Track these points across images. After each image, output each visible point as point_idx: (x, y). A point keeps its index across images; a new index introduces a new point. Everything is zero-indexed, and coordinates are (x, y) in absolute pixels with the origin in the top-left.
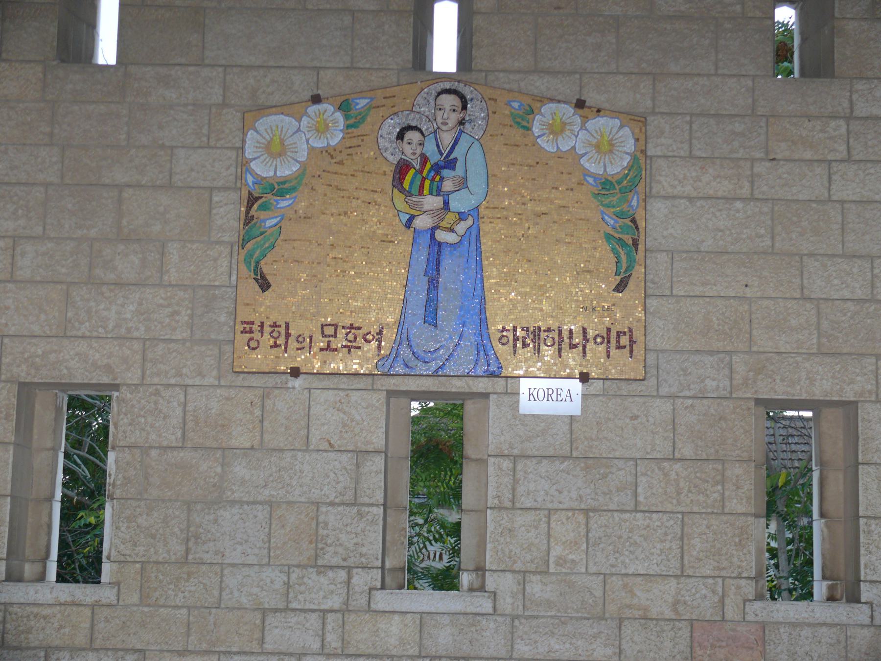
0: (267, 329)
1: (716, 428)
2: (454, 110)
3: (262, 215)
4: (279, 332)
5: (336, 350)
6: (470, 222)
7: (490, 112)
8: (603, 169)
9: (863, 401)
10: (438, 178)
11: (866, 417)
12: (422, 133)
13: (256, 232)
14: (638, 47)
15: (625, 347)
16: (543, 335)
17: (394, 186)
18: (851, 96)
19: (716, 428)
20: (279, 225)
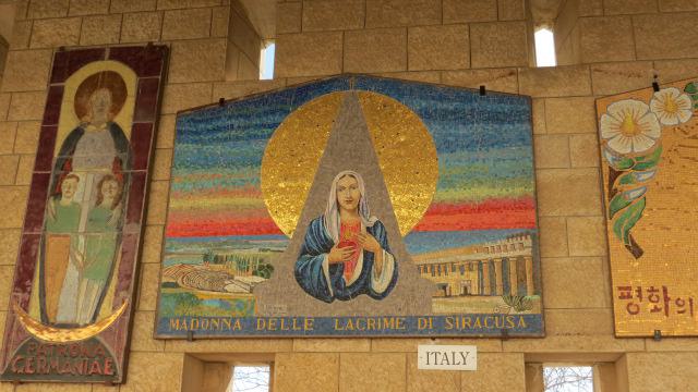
0: (645, 294)
3: (625, 187)
4: (657, 296)
13: (621, 203)
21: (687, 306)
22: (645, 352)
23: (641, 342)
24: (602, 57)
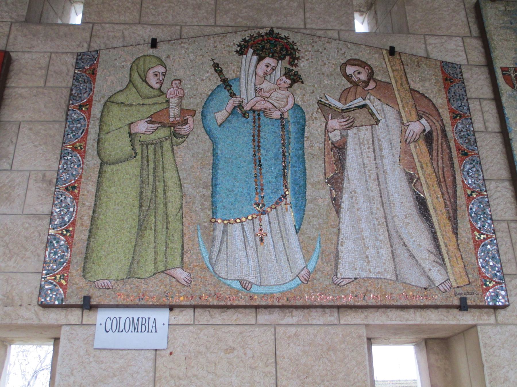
1: (325, 360)
9: (482, 324)
11: (488, 342)
14: (234, 7)
18: (426, 47)
19: (325, 360)
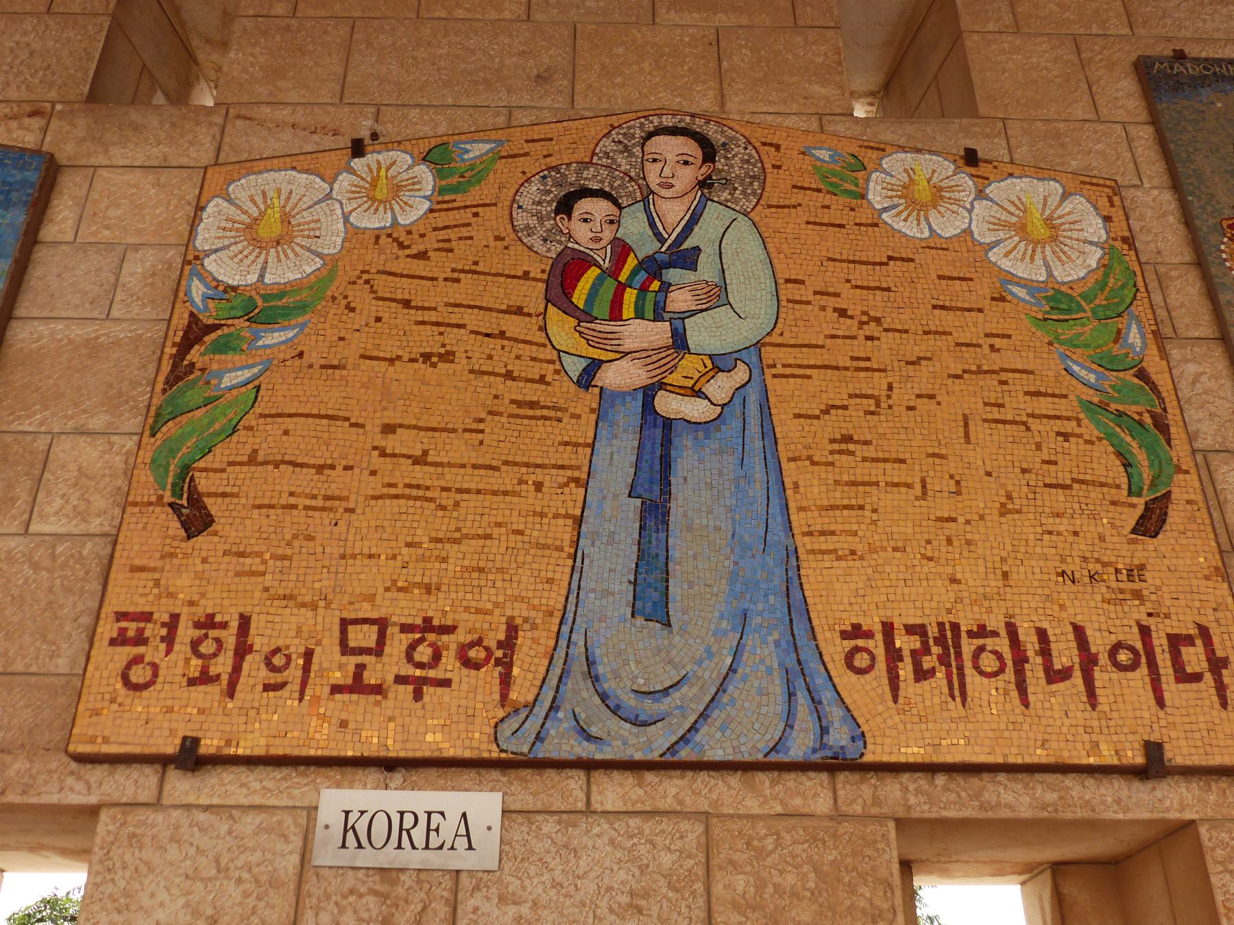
0: (185, 633)
2: (686, 163)
5: (378, 690)
6: (741, 374)
7: (768, 166)
8: (1043, 271)
10: (655, 285)
12: (615, 202)
13: (194, 396)
15: (1197, 677)
16: (968, 646)
17: (548, 301)
20: (256, 383)
21: (294, 673)
22: (156, 804)
23: (147, 777)
24: (262, 91)
